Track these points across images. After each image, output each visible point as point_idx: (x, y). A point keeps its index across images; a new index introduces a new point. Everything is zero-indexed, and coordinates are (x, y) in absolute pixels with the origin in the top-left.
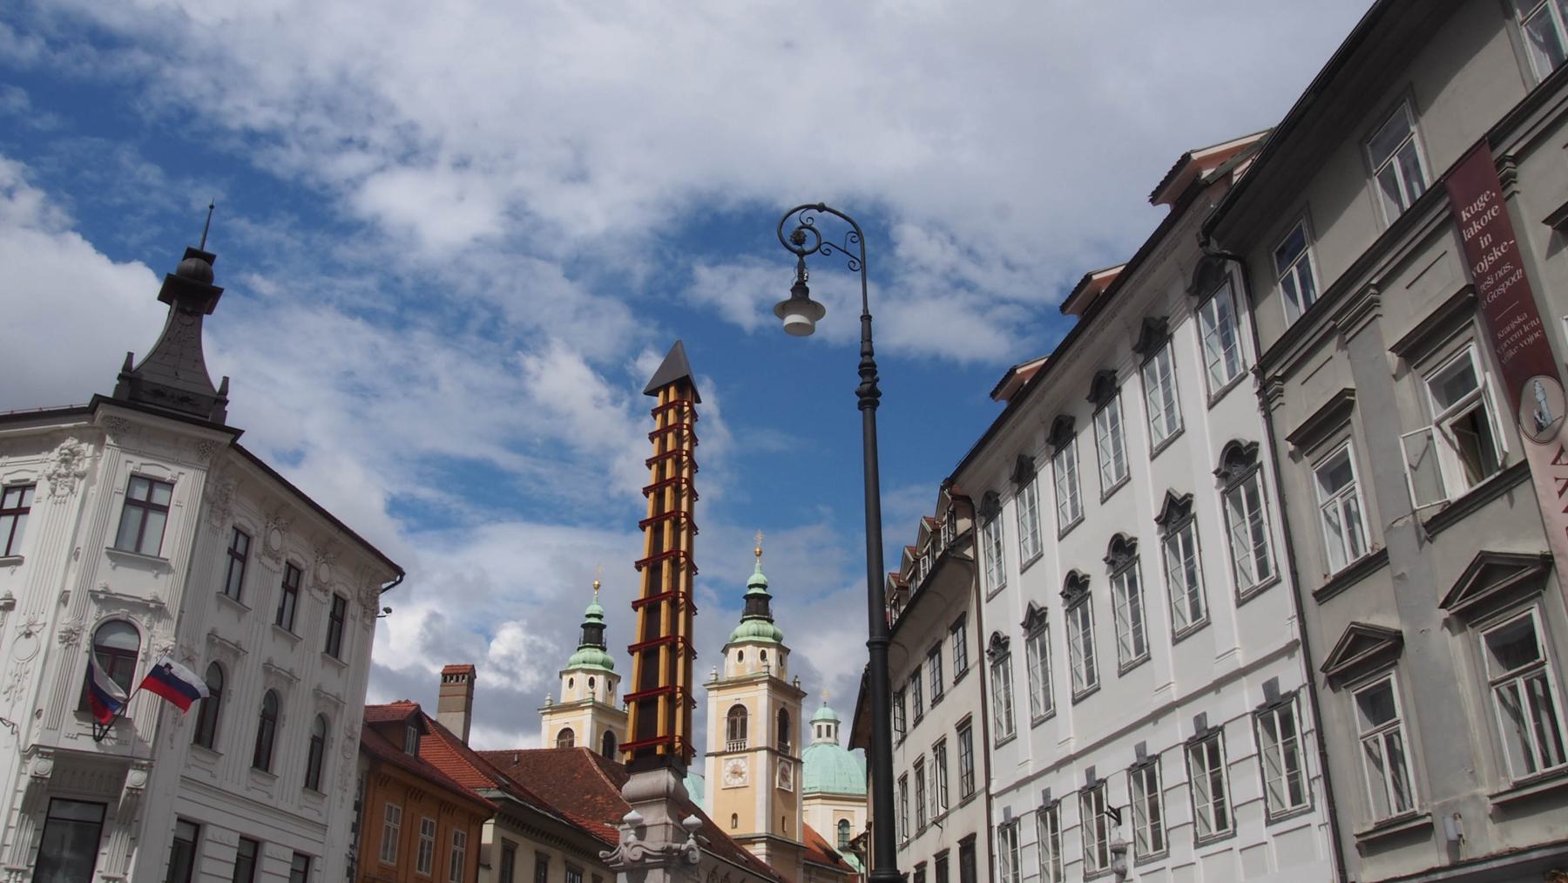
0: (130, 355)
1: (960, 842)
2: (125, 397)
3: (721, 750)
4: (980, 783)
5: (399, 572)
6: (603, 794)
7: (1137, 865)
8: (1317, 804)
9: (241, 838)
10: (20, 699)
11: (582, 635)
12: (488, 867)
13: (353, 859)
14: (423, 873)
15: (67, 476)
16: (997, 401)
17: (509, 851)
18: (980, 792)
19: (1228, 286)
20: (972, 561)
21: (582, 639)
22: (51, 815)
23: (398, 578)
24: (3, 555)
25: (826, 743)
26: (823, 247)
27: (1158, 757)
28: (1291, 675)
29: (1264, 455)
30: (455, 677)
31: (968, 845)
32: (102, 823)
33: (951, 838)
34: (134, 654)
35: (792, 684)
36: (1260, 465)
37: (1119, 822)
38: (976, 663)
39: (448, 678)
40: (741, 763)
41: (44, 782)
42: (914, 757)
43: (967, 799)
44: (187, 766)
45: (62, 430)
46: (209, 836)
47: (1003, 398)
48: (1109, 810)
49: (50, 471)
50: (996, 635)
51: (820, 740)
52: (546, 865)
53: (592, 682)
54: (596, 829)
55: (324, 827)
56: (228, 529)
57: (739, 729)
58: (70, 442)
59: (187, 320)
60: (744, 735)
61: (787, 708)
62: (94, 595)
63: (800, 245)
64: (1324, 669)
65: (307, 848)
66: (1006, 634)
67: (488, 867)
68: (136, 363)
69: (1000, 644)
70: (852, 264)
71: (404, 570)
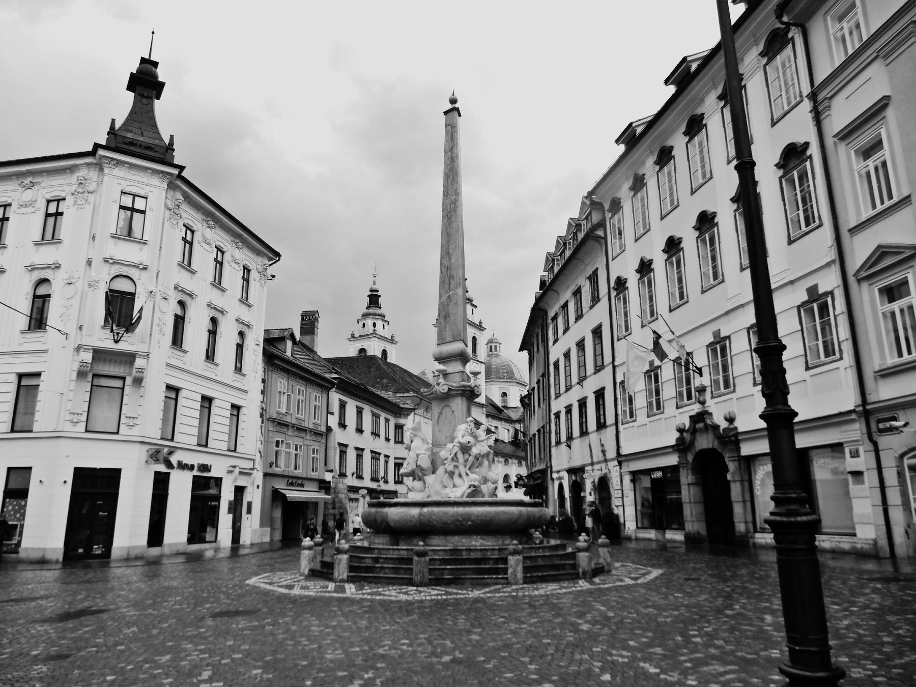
0: (113, 121)
2: (113, 145)
4: (608, 359)
5: (278, 255)
7: (713, 397)
8: (845, 355)
10: (69, 320)
12: (332, 414)
13: (263, 409)
14: (299, 416)
15: (83, 193)
17: (343, 405)
18: (608, 365)
19: (790, 46)
20: (603, 238)
22: (94, 384)
24: (50, 238)
27: (728, 337)
28: (830, 281)
29: (814, 150)
31: (600, 395)
32: (123, 389)
33: (589, 389)
34: (134, 294)
36: (810, 157)
37: (701, 375)
38: (603, 297)
41: (88, 365)
42: (564, 350)
43: (598, 369)
44: (169, 358)
45: (76, 166)
47: (622, 143)
48: (694, 368)
49: (73, 190)
50: (619, 279)
52: (361, 413)
53: (374, 325)
55: (246, 392)
56: (181, 225)
58: (83, 172)
59: (145, 101)
62: (106, 261)
64: (855, 275)
65: (238, 402)
66: (625, 277)
67: (332, 414)
68: (117, 126)
69: (621, 284)
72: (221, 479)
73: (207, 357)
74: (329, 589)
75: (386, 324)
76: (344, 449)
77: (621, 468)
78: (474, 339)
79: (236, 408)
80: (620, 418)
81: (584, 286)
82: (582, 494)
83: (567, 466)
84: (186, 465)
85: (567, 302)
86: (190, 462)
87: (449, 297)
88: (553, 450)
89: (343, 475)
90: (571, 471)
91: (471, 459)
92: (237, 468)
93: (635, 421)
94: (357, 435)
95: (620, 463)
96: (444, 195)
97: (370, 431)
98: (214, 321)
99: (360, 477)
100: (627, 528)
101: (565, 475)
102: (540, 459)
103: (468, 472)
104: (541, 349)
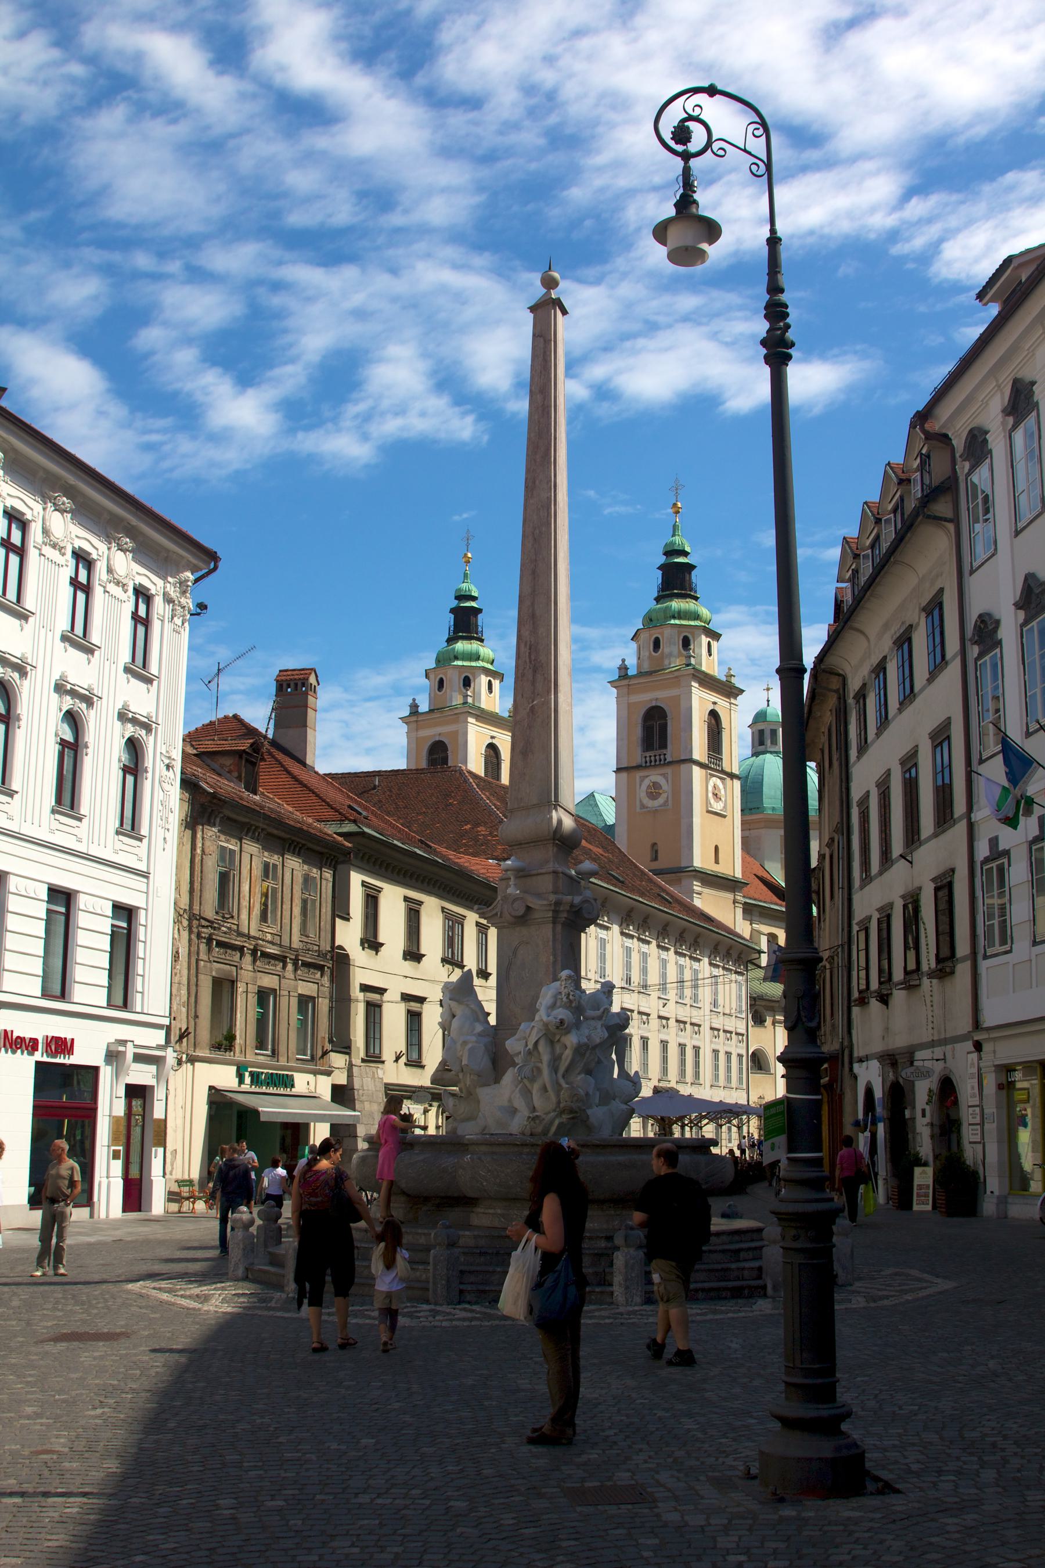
1: (933, 880)
3: (635, 765)
5: (212, 556)
6: (485, 823)
9: (49, 889)
11: (452, 623)
16: (985, 304)
18: (960, 819)
21: (452, 629)
23: (212, 566)
25: (771, 753)
26: (716, 146)
30: (292, 685)
31: (944, 887)
35: (724, 679)
38: (954, 657)
39: (285, 686)
40: (661, 780)
42: (878, 773)
46: (12, 889)
47: (992, 300)
51: (762, 748)
52: (418, 912)
54: (480, 867)
55: (145, 875)
57: (656, 738)
60: (663, 745)
61: (717, 709)
63: (685, 144)
70: (754, 168)
71: (219, 554)
72: (96, 1069)
73: (59, 800)
74: (273, 1304)
75: (496, 683)
76: (374, 997)
77: (980, 1058)
78: (714, 714)
79: (125, 912)
80: (981, 941)
81: (918, 624)
82: (907, 1113)
83: (878, 1047)
84: (21, 1040)
85: (885, 657)
86: (28, 1035)
87: (532, 709)
88: (856, 1010)
89: (373, 1057)
90: (891, 1060)
91: (568, 1054)
92: (130, 1044)
93: (1010, 951)
94: (408, 967)
95: (978, 1046)
96: (526, 487)
97: (439, 955)
98: (72, 718)
99: (416, 1063)
100: (988, 1192)
101: (875, 1065)
102: (833, 1026)
103: (562, 1081)
104: (836, 764)
